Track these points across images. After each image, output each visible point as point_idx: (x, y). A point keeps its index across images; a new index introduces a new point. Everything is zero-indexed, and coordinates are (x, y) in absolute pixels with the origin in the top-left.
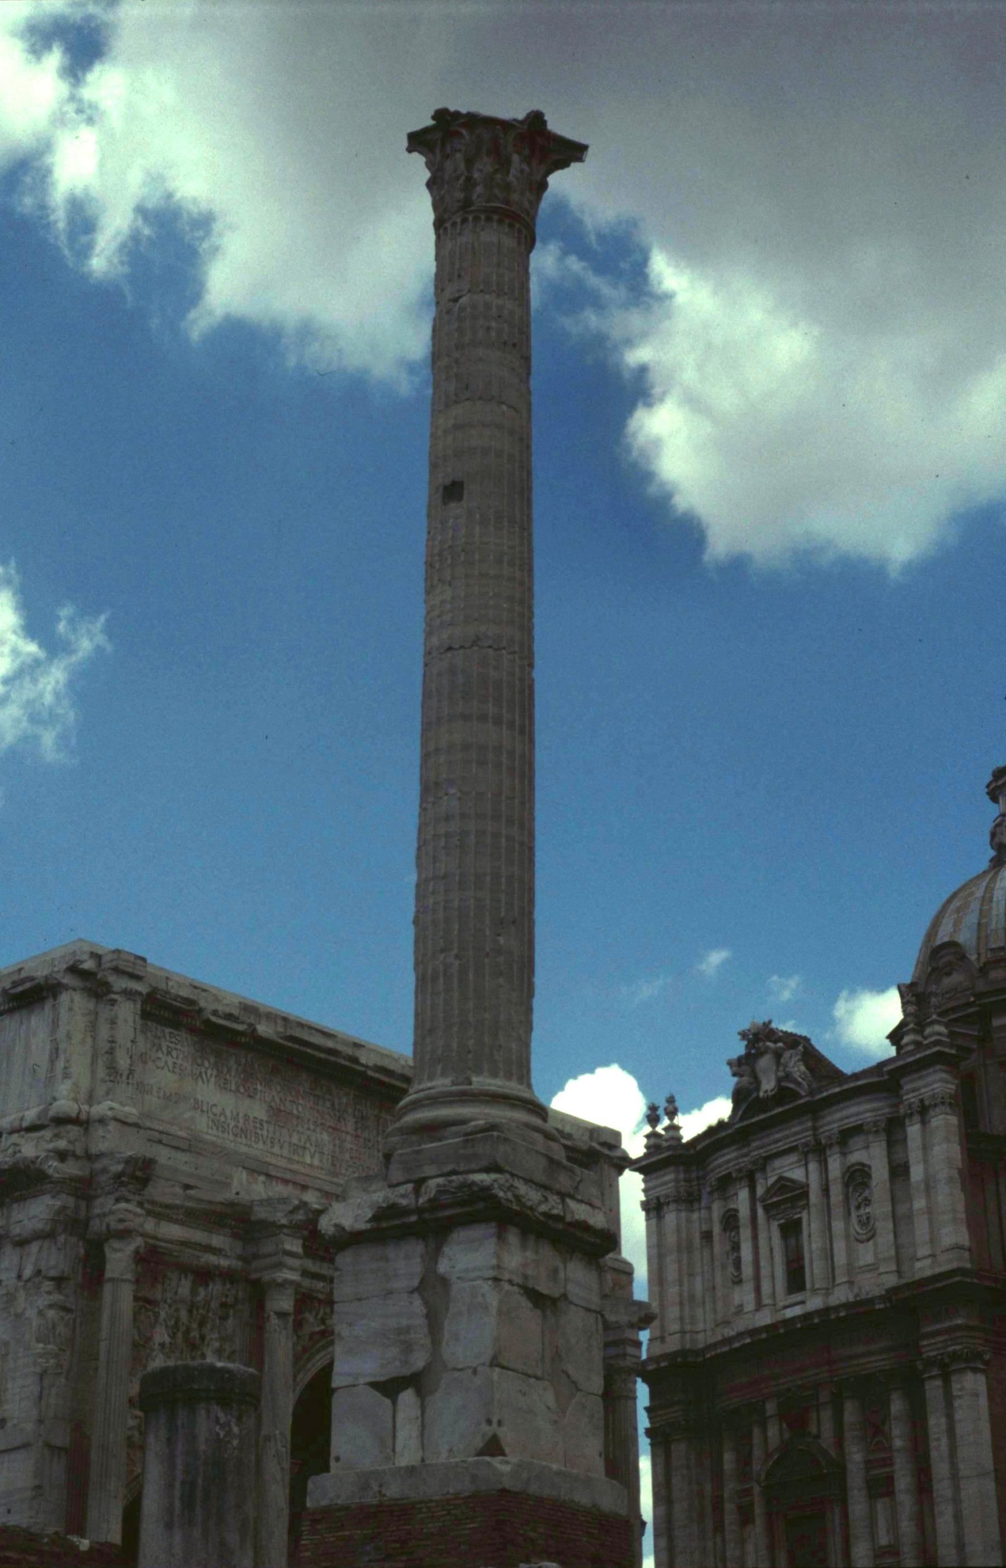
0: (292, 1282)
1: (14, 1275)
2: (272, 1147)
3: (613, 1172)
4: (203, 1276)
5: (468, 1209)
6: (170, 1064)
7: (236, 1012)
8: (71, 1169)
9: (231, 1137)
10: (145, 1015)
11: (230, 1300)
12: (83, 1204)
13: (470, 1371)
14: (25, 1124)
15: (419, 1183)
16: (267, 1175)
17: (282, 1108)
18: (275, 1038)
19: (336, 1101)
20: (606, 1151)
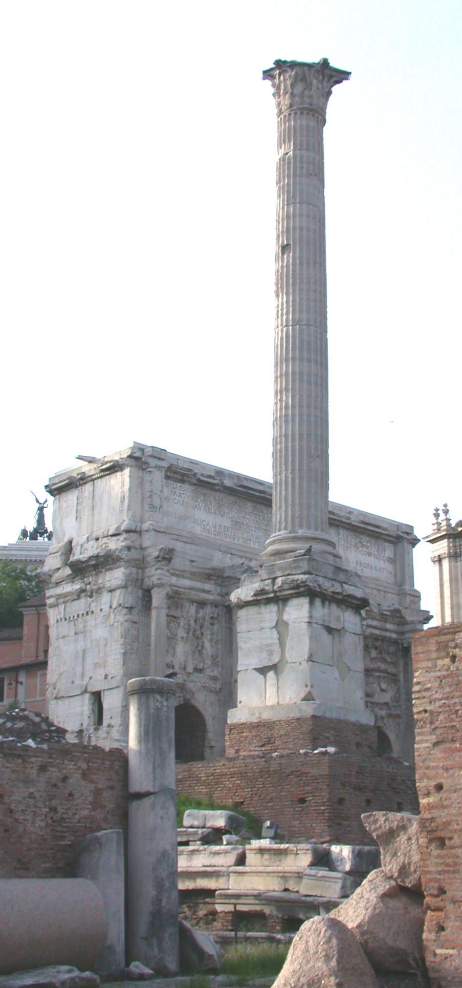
1: (109, 606)
2: (234, 540)
3: (410, 546)
4: (201, 604)
5: (296, 591)
6: (181, 502)
7: (213, 474)
8: (134, 554)
9: (213, 536)
10: (167, 477)
11: (215, 616)
12: (140, 571)
13: (298, 664)
14: (110, 533)
15: (274, 579)
16: (232, 554)
17: (238, 520)
19: (266, 516)
20: (405, 536)
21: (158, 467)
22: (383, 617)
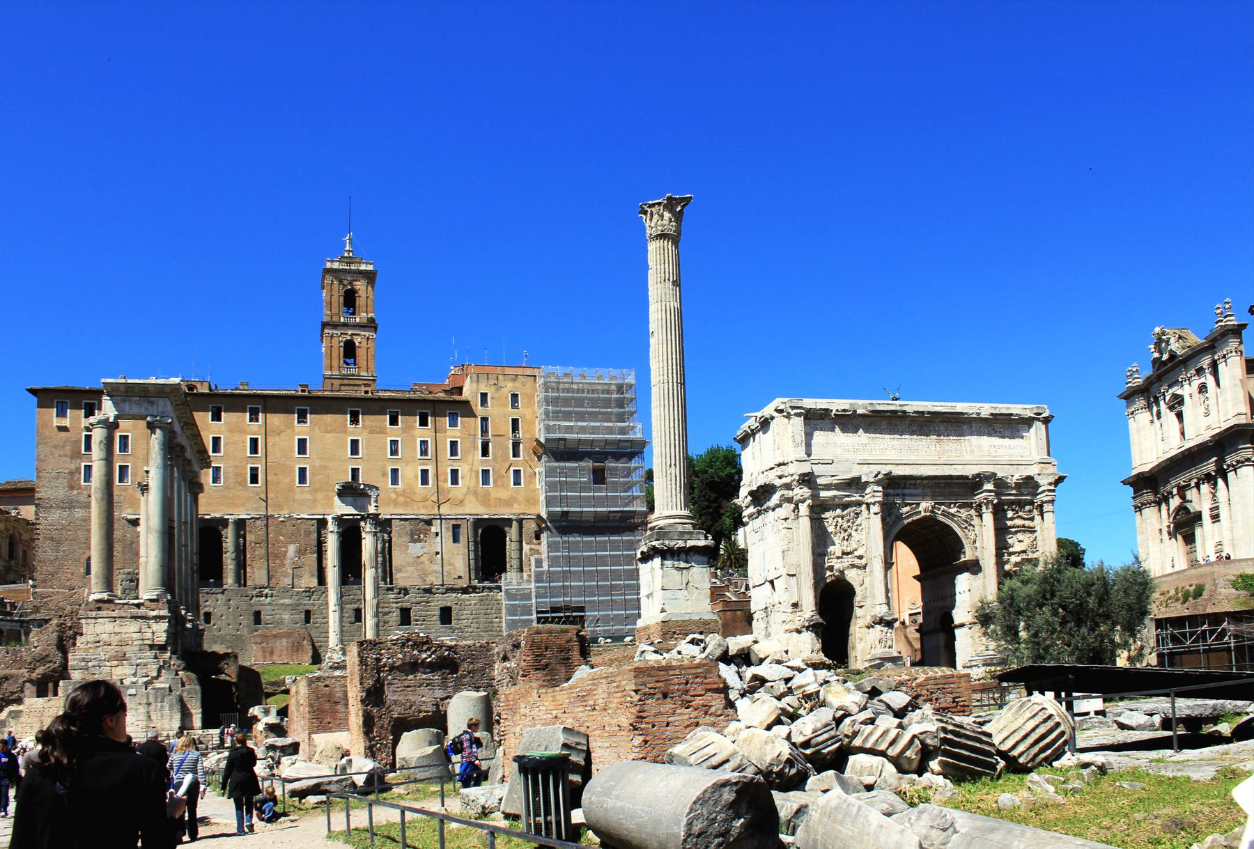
0: (878, 502)
8: (784, 480)
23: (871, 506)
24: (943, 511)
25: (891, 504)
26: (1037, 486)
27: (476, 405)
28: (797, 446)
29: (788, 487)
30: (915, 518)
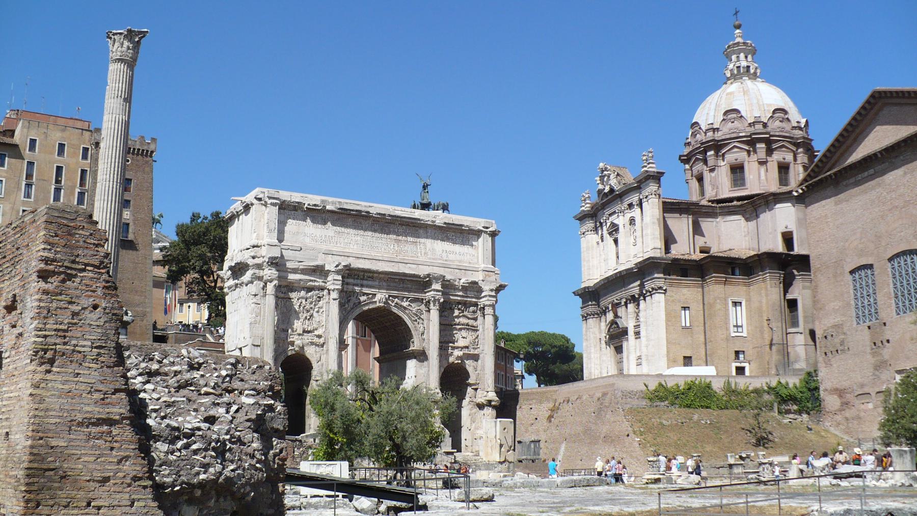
0: (337, 289)
4: (309, 289)
8: (257, 261)
18: (334, 209)
19: (364, 226)
21: (273, 204)
22: (464, 289)
23: (331, 292)
24: (397, 303)
25: (350, 292)
26: (480, 290)
27: (25, 150)
28: (270, 231)
29: (259, 267)
30: (371, 306)
